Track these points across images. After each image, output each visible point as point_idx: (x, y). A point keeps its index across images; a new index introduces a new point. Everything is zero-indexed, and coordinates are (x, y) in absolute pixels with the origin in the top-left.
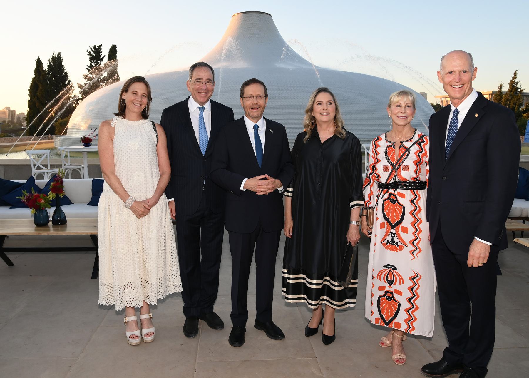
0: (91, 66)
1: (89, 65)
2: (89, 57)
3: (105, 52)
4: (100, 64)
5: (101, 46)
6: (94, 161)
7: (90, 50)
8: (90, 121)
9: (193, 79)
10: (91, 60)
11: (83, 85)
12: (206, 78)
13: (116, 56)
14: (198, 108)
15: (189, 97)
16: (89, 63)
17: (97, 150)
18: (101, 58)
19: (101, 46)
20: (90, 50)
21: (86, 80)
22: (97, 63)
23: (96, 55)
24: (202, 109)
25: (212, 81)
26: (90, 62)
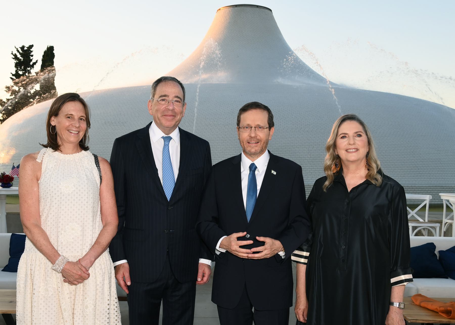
0: (17, 75)
1: (14, 73)
2: (14, 61)
3: (37, 56)
4: (29, 72)
5: (31, 46)
6: (13, 208)
7: (15, 52)
8: (13, 152)
9: (157, 97)
10: (17, 65)
11: (5, 100)
12: (174, 95)
13: (53, 63)
14: (163, 137)
15: (151, 122)
17: (17, 193)
18: (31, 63)
19: (31, 46)
20: (15, 52)
21: (10, 94)
22: (25, 70)
23: (24, 59)
24: (167, 139)
25: (182, 100)
26: (15, 69)
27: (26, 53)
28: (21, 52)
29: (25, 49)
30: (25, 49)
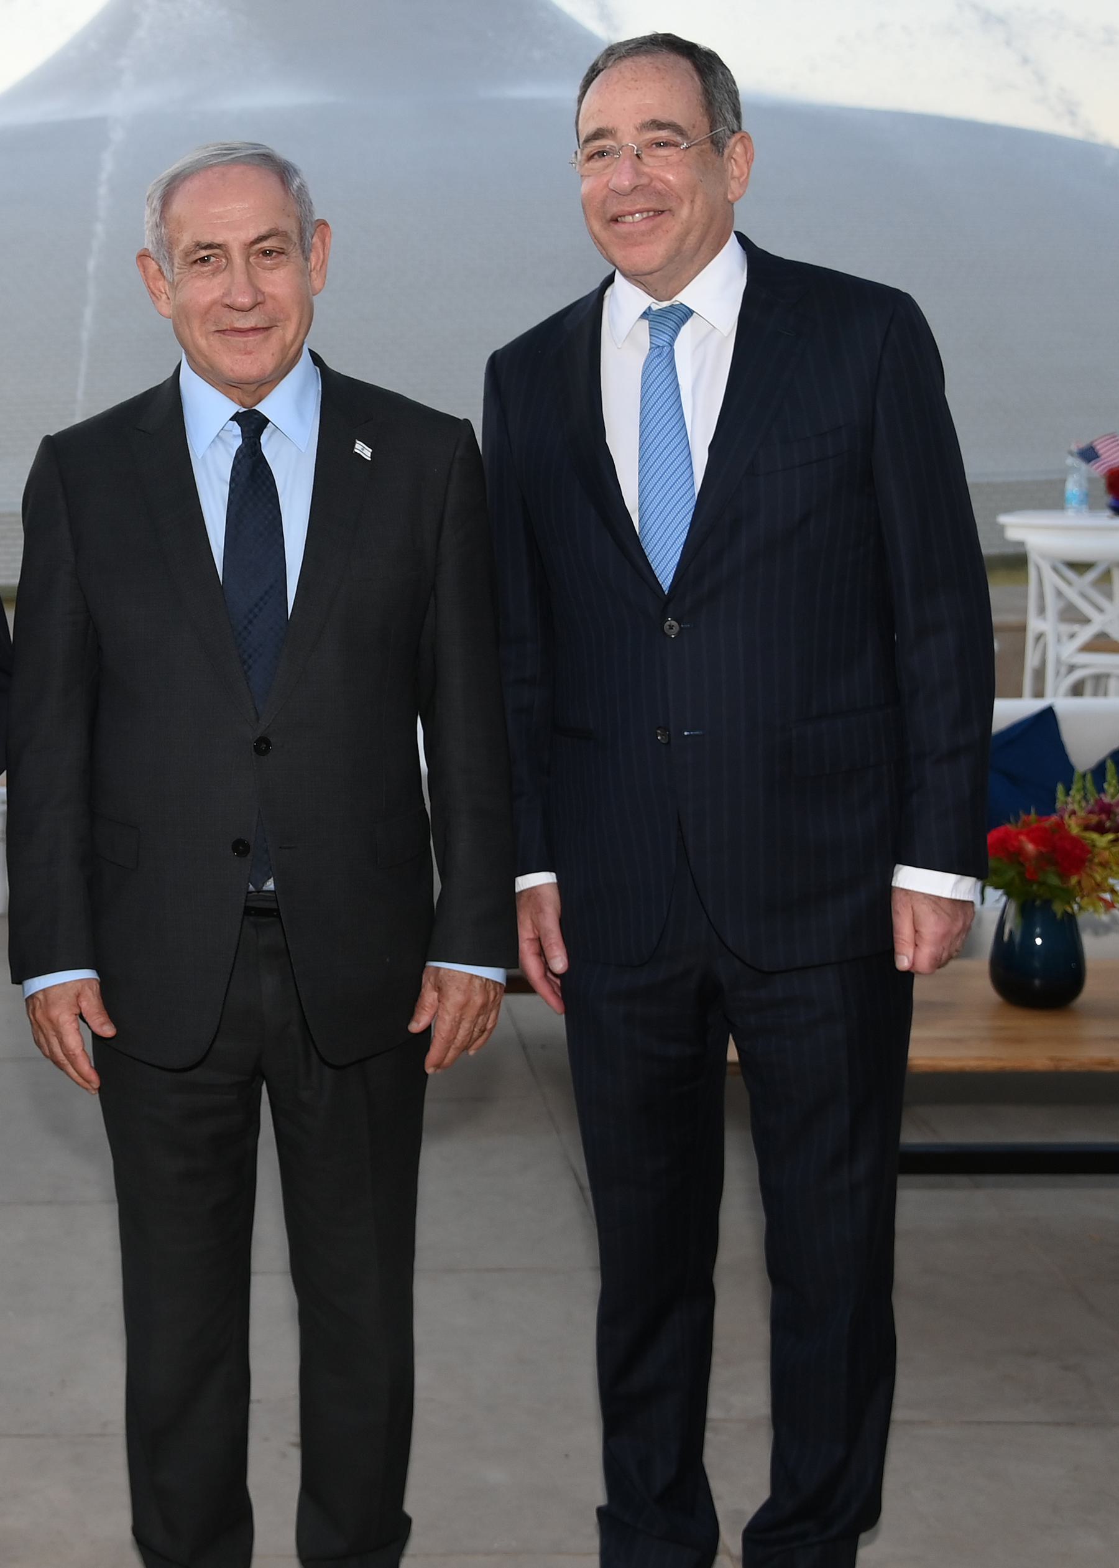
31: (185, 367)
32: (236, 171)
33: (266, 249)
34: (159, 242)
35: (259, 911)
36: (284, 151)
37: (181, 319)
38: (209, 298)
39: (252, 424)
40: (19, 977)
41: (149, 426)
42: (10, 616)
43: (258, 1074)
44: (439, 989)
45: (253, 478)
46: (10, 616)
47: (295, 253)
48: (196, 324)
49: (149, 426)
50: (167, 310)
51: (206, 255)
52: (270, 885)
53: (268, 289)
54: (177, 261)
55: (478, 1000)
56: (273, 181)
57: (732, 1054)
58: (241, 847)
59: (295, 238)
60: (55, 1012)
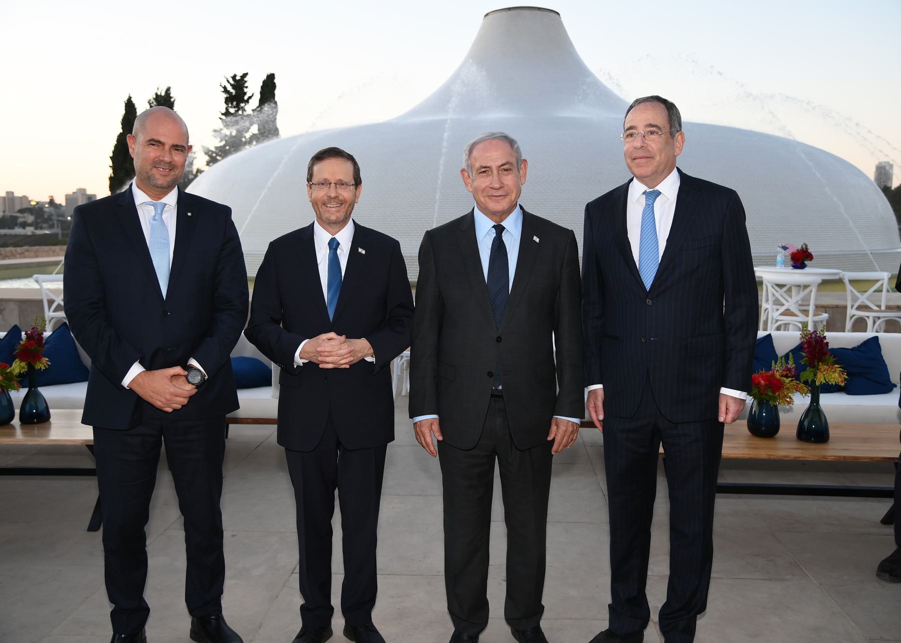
0: (227, 114)
1: (224, 111)
3: (253, 88)
5: (245, 75)
10: (227, 101)
16: (223, 107)
19: (245, 75)
23: (236, 94)
26: (225, 106)
27: (239, 84)
28: (232, 82)
29: (238, 78)
30: (238, 78)
31: (476, 209)
32: (494, 142)
33: (506, 168)
34: (468, 166)
35: (496, 396)
36: (512, 136)
37: (475, 192)
38: (484, 186)
39: (499, 229)
40: (412, 416)
41: (463, 228)
42: (414, 292)
43: (494, 452)
44: (557, 425)
45: (499, 247)
46: (414, 292)
47: (515, 170)
48: (480, 193)
49: (463, 228)
50: (471, 190)
51: (485, 170)
52: (500, 388)
53: (505, 182)
54: (474, 172)
55: (570, 429)
56: (507, 145)
57: (661, 450)
58: (490, 374)
59: (515, 165)
60: (423, 429)
